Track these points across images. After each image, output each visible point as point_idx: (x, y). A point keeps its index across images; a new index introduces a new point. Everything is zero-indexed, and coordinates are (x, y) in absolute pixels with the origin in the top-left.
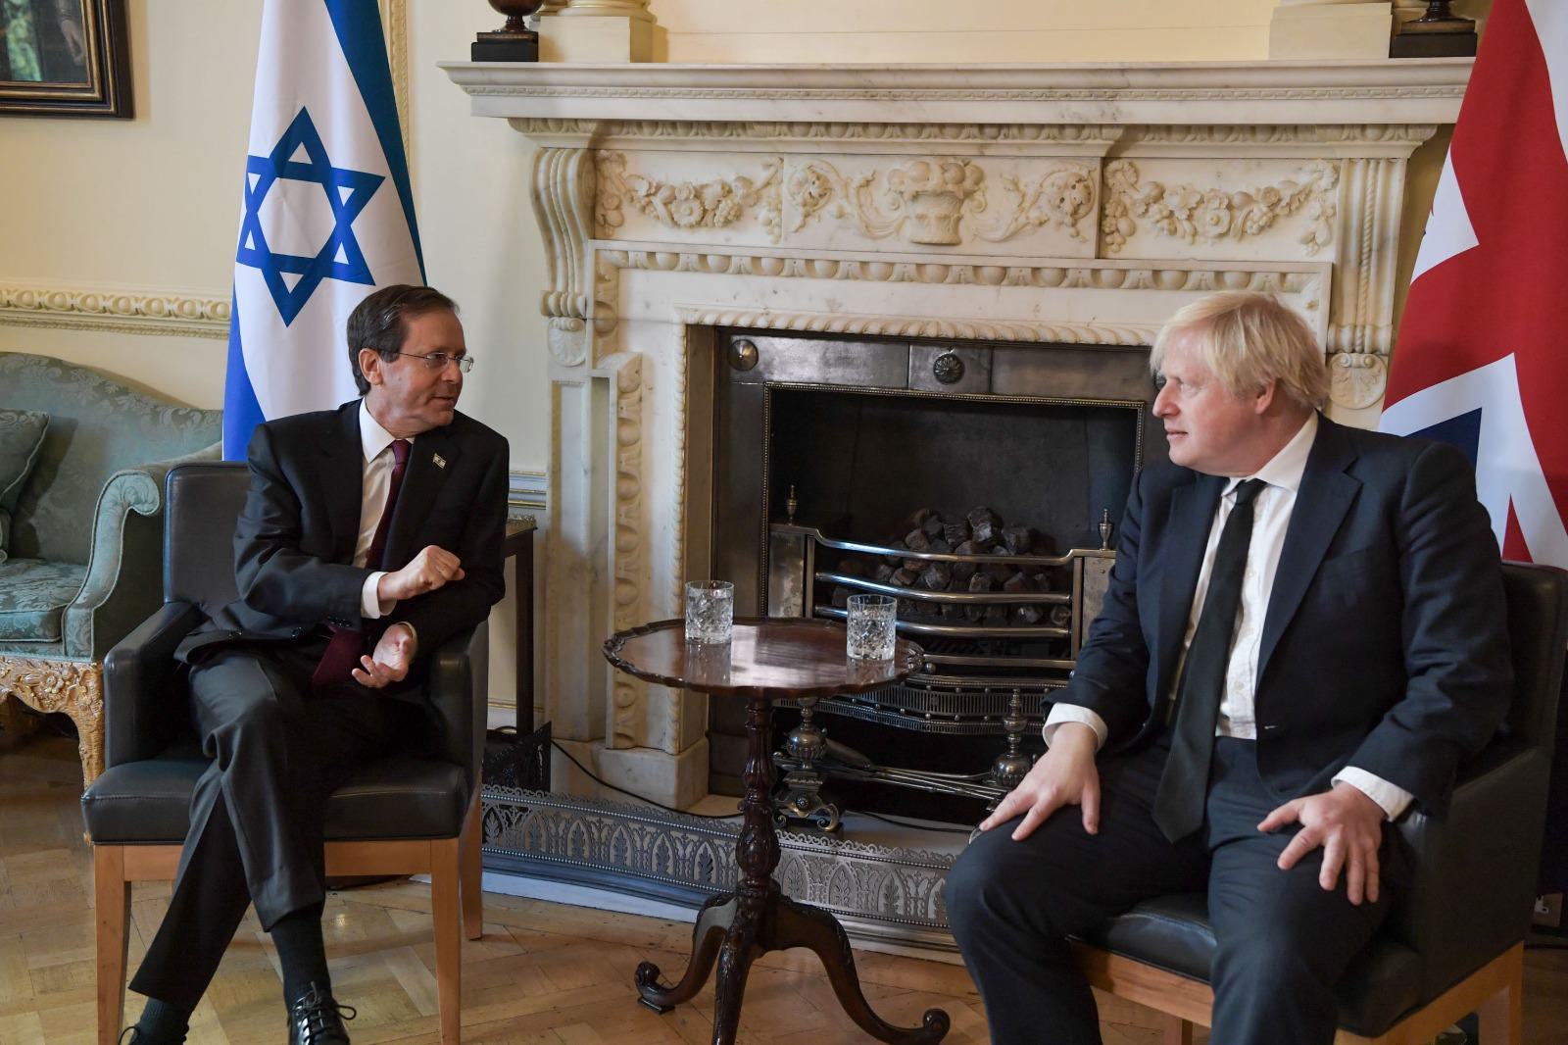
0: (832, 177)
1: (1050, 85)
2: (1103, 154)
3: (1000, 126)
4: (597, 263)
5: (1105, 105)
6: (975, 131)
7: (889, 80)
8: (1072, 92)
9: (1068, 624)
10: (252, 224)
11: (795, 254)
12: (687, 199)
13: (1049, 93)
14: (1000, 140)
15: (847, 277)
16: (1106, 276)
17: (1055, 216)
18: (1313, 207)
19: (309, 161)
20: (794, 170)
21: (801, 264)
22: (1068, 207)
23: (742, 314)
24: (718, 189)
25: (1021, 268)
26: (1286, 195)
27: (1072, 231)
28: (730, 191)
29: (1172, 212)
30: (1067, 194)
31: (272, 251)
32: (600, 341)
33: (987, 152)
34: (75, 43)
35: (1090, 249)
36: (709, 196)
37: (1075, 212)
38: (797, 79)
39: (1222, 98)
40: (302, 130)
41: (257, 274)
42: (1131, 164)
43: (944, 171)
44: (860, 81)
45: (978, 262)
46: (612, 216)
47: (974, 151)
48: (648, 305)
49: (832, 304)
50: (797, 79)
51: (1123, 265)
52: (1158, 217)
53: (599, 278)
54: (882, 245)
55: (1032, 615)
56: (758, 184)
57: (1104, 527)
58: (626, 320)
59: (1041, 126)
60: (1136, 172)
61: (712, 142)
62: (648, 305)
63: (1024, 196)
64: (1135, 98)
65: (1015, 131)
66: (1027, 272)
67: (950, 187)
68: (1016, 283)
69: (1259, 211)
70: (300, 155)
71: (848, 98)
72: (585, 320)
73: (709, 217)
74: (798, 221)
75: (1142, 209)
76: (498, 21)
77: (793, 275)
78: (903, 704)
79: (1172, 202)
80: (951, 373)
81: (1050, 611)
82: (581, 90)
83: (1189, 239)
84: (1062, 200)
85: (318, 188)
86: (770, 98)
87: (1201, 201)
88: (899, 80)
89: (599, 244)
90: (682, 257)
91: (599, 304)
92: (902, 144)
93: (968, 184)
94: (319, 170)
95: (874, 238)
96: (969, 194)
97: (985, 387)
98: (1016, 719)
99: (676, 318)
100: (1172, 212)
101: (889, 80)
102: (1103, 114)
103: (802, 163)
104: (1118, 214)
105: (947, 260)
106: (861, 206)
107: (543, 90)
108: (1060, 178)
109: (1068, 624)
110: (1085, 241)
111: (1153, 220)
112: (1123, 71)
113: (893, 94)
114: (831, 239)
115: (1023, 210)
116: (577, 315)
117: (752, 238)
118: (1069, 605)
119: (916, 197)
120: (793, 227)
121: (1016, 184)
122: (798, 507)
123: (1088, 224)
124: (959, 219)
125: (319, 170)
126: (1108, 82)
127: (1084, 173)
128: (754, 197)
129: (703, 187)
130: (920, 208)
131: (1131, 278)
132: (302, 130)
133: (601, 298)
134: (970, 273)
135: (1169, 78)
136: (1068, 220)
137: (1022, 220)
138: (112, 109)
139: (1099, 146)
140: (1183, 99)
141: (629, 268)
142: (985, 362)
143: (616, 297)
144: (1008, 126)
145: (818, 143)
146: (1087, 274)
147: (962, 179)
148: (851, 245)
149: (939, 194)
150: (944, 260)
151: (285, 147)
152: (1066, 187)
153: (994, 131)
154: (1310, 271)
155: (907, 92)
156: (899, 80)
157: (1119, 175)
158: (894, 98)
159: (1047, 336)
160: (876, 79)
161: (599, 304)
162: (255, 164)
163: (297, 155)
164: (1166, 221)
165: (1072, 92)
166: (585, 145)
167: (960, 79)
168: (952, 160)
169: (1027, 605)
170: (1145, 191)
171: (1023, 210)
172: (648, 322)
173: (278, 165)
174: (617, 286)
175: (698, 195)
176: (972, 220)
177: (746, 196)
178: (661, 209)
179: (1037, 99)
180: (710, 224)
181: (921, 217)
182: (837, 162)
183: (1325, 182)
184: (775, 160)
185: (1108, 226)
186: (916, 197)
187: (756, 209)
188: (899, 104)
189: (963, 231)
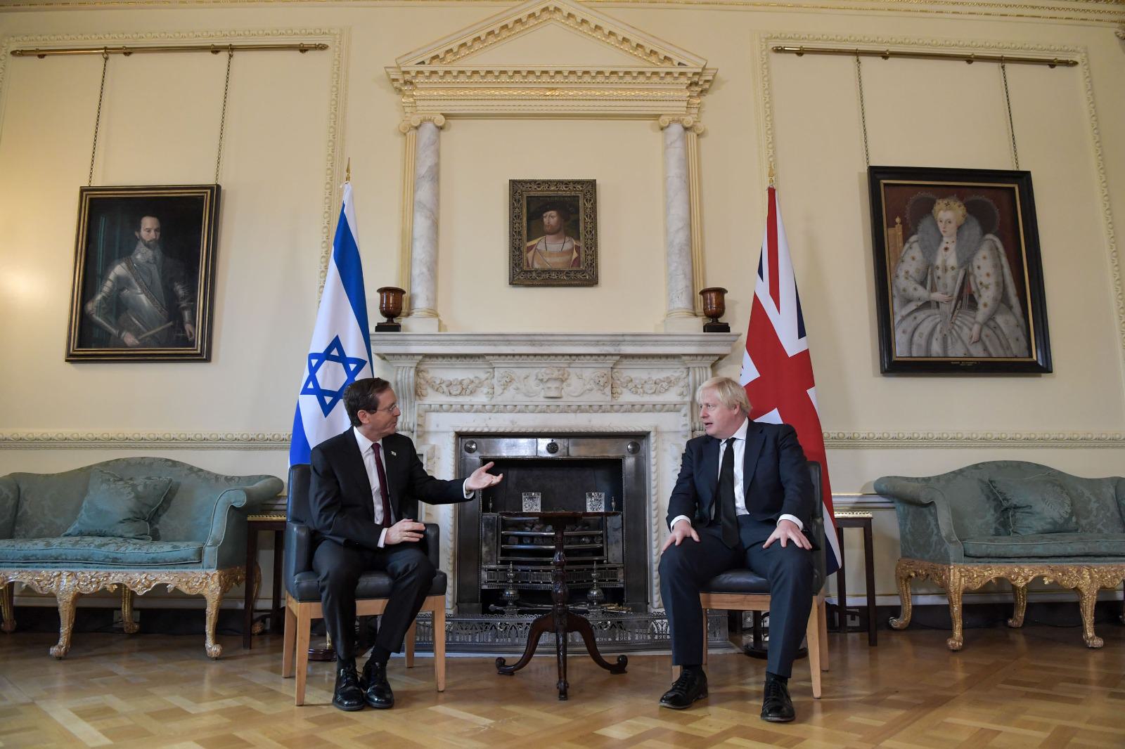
0: (513, 376)
1: (598, 340)
2: (611, 366)
4: (418, 410)
5: (616, 347)
7: (541, 338)
8: (606, 343)
9: (602, 542)
10: (312, 378)
12: (456, 384)
13: (597, 343)
14: (577, 361)
15: (519, 412)
18: (682, 383)
19: (337, 355)
22: (601, 383)
26: (673, 379)
28: (473, 382)
29: (636, 386)
31: (322, 387)
32: (420, 439)
34: (190, 332)
35: (609, 398)
36: (465, 383)
38: (506, 338)
39: (654, 345)
40: (336, 343)
41: (314, 398)
44: (530, 339)
46: (424, 392)
48: (438, 426)
49: (512, 422)
50: (506, 338)
53: (419, 416)
55: (587, 540)
57: (613, 503)
58: (428, 432)
62: (438, 426)
67: (561, 377)
68: (582, 411)
69: (665, 384)
70: (335, 352)
72: (413, 432)
73: (464, 391)
74: (501, 391)
76: (384, 320)
77: (498, 412)
78: (541, 579)
80: (552, 448)
81: (594, 537)
82: (419, 342)
85: (341, 365)
86: (495, 345)
87: (645, 382)
88: (545, 338)
89: (420, 402)
90: (454, 406)
91: (418, 425)
92: (540, 363)
93: (566, 376)
94: (342, 359)
96: (566, 379)
97: (566, 454)
98: (597, 572)
99: (451, 429)
100: (636, 386)
101: (541, 338)
102: (615, 351)
103: (502, 371)
105: (558, 404)
106: (525, 385)
107: (404, 342)
108: (599, 374)
109: (602, 542)
110: (607, 396)
112: (623, 335)
113: (541, 343)
114: (514, 398)
116: (409, 430)
117: (481, 398)
118: (601, 535)
120: (499, 393)
122: (493, 505)
123: (608, 390)
125: (342, 359)
126: (618, 339)
127: (606, 372)
128: (481, 384)
129: (463, 380)
130: (549, 385)
132: (336, 343)
133: (420, 423)
134: (566, 408)
135: (637, 338)
138: (205, 357)
140: (642, 345)
141: (431, 411)
142: (566, 445)
143: (424, 423)
147: (563, 375)
148: (521, 399)
149: (556, 379)
150: (555, 403)
151: (329, 349)
154: (684, 404)
155: (546, 343)
156: (545, 338)
160: (536, 338)
161: (418, 425)
162: (312, 356)
163: (334, 351)
165: (606, 343)
166: (415, 365)
167: (566, 338)
169: (585, 536)
172: (436, 432)
173: (326, 356)
174: (425, 419)
177: (480, 383)
178: (446, 389)
179: (592, 345)
181: (549, 388)
182: (515, 370)
183: (685, 375)
184: (491, 370)
187: (482, 389)
188: (543, 347)
189: (563, 393)
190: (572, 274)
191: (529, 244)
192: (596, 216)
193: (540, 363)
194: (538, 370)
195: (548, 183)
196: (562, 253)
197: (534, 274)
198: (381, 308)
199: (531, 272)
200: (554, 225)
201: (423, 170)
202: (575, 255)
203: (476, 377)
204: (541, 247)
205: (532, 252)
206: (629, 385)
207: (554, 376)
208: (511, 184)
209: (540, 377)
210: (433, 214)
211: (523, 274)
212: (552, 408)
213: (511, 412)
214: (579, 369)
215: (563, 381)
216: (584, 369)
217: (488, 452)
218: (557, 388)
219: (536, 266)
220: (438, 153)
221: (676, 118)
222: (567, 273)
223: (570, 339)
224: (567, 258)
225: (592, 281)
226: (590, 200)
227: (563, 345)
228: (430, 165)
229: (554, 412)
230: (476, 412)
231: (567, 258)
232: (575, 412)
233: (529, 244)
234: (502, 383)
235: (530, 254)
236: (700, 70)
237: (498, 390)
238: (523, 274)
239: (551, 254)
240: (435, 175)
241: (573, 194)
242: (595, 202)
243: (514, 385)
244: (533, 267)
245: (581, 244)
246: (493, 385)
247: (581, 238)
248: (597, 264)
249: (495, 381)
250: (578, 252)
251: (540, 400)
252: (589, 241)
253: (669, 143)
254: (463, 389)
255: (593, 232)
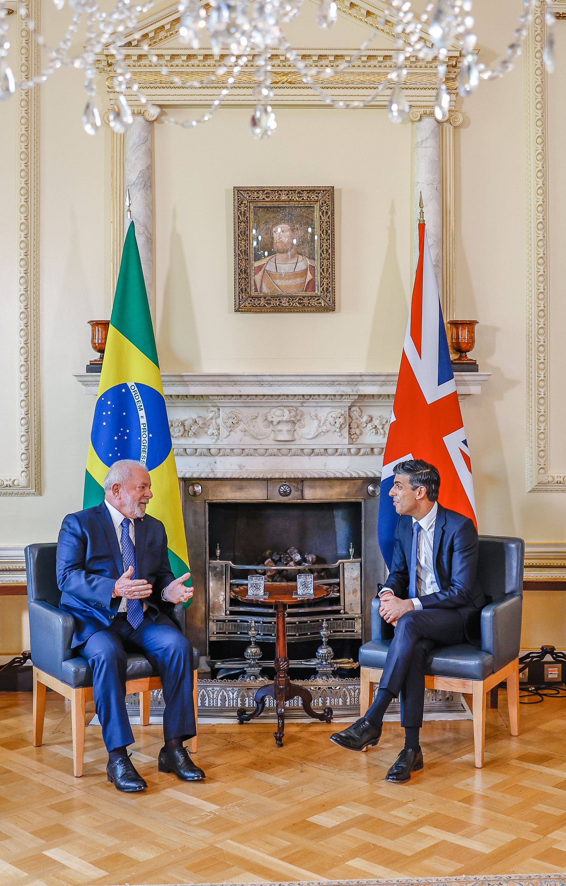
1: (333, 380)
3: (311, 395)
6: (301, 397)
7: (270, 379)
11: (226, 447)
13: (332, 383)
16: (353, 451)
17: (333, 429)
20: (223, 413)
21: (228, 451)
22: (338, 425)
23: (202, 473)
24: (191, 421)
25: (320, 449)
27: (339, 434)
28: (196, 422)
29: (376, 426)
30: (337, 420)
33: (304, 405)
35: (346, 441)
36: (187, 423)
37: (341, 427)
42: (359, 408)
43: (290, 413)
45: (302, 447)
47: (299, 404)
49: (241, 467)
50: (232, 379)
51: (360, 446)
52: (371, 428)
54: (263, 442)
56: (208, 419)
59: (327, 395)
60: (361, 411)
61: (185, 403)
63: (320, 421)
64: (364, 385)
65: (317, 397)
66: (322, 451)
67: (293, 419)
71: (252, 385)
74: (228, 434)
75: (365, 425)
79: (376, 422)
83: (382, 436)
84: (336, 423)
93: (298, 418)
95: (259, 439)
96: (298, 421)
101: (270, 379)
103: (228, 410)
104: (356, 427)
110: (344, 438)
111: (369, 429)
112: (361, 375)
113: (270, 384)
115: (320, 427)
117: (204, 441)
119: (279, 423)
121: (316, 416)
124: (295, 430)
126: (354, 379)
127: (343, 412)
129: (184, 421)
130: (279, 427)
131: (362, 452)
136: (338, 430)
137: (320, 430)
139: (347, 402)
144: (314, 395)
145: (235, 402)
146: (346, 451)
148: (249, 443)
149: (287, 422)
152: (337, 418)
153: (308, 397)
157: (355, 412)
158: (271, 386)
159: (332, 476)
164: (374, 430)
167: (298, 378)
168: (291, 408)
170: (365, 418)
171: (320, 427)
175: (183, 424)
176: (300, 431)
177: (204, 424)
180: (187, 435)
181: (280, 431)
182: (241, 409)
185: (353, 431)
186: (279, 423)
188: (273, 388)
190: (306, 301)
191: (257, 264)
192: (333, 231)
193: (270, 402)
194: (265, 411)
195: (279, 191)
196: (296, 275)
197: (263, 302)
198: (93, 343)
199: (259, 298)
200: (286, 239)
201: (133, 173)
202: (309, 276)
203: (200, 417)
204: (270, 267)
205: (261, 273)
206: (369, 425)
207: (285, 418)
208: (236, 192)
209: (270, 419)
210: (146, 228)
211: (250, 299)
212: (285, 451)
213: (239, 455)
214: (313, 409)
215: (294, 423)
216: (320, 408)
217: (213, 496)
218: (288, 431)
219: (265, 290)
220: (151, 153)
221: (428, 110)
222: (300, 299)
223: (302, 379)
224: (299, 281)
225: (330, 308)
226: (327, 213)
227: (294, 385)
228: (142, 169)
229: (286, 455)
230: (201, 455)
231: (299, 281)
232: (310, 455)
233: (257, 264)
234: (228, 425)
235: (258, 277)
236: (457, 54)
237: (224, 432)
238: (250, 299)
239: (281, 274)
240: (148, 181)
241: (307, 204)
242: (333, 214)
243: (242, 426)
244: (261, 291)
245: (317, 264)
246: (219, 425)
247: (316, 258)
248: (333, 289)
249: (220, 421)
250: (314, 275)
251: (269, 442)
252: (325, 261)
253: (419, 140)
254: (185, 430)
255: (330, 251)
